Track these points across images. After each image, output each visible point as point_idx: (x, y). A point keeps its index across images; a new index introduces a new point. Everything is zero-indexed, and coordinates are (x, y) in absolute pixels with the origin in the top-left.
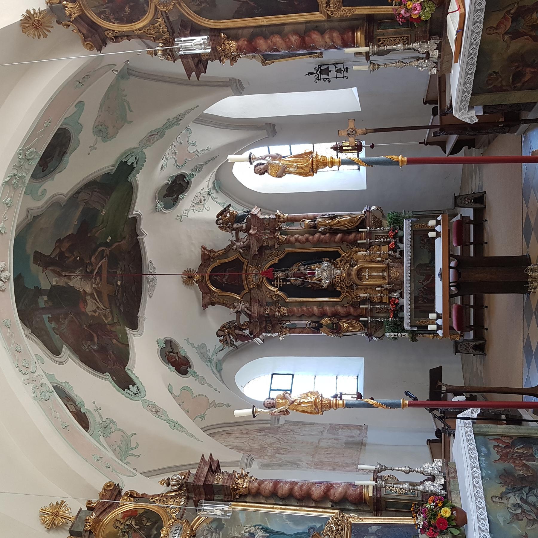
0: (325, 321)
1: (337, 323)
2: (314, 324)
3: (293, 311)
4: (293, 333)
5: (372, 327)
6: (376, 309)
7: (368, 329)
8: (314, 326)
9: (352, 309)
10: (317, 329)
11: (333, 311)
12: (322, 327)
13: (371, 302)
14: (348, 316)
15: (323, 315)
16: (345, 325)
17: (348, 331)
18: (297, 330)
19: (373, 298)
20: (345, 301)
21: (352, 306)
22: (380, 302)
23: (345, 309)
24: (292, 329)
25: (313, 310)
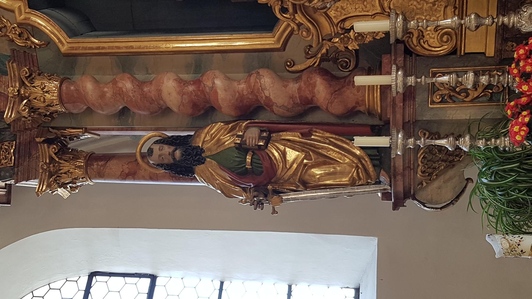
0: (217, 136)
1: (259, 151)
2: (167, 149)
3: (79, 97)
4: (101, 176)
5: (409, 167)
6: (433, 88)
7: (393, 176)
8: (168, 160)
9: (321, 90)
10: (185, 162)
11: (241, 97)
12: (202, 161)
13: (408, 52)
14: (301, 116)
15: (204, 111)
16: (292, 155)
17: (306, 185)
18: (114, 166)
19: (421, 36)
20: (295, 51)
21: (325, 73)
22: (454, 52)
23: (293, 87)
24: (96, 163)
25: (159, 91)
